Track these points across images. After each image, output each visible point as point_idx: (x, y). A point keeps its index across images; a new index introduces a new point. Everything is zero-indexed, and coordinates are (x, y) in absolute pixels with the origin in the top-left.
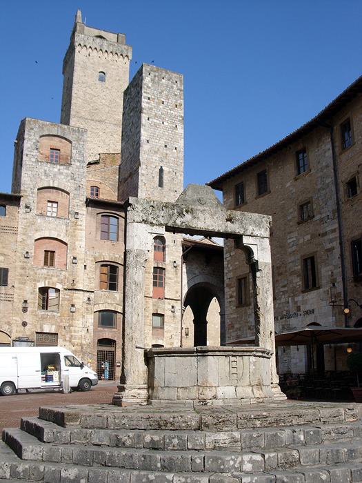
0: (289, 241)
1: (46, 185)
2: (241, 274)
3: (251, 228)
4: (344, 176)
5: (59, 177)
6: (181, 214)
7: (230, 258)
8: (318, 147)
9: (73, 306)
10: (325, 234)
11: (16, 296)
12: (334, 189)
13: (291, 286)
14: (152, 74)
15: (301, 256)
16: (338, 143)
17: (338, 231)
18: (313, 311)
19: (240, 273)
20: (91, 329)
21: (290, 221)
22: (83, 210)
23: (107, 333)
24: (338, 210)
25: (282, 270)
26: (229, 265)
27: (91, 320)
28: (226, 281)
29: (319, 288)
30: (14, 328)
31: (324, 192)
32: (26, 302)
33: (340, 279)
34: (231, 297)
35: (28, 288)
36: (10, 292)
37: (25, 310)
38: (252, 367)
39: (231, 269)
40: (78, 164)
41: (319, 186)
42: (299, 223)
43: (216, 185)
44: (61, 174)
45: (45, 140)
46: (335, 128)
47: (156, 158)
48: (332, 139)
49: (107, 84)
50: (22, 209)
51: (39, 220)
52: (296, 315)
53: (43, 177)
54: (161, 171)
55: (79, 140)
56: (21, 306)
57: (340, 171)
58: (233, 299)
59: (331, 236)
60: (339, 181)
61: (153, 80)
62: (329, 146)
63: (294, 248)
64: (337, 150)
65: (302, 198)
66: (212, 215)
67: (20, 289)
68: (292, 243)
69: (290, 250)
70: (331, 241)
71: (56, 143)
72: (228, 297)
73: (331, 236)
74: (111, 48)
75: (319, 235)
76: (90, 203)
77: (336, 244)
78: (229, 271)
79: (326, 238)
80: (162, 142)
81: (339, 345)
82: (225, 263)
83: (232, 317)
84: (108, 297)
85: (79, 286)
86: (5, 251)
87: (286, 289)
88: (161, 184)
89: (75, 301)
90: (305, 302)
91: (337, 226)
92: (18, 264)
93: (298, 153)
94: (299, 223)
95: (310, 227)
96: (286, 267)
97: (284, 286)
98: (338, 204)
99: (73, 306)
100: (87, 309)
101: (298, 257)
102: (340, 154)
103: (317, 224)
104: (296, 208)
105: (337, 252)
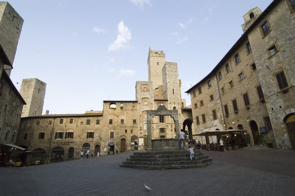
1: (144, 97)
3: (173, 113)
4: (221, 88)
5: (146, 95)
6: (158, 112)
9: (153, 128)
10: (217, 104)
11: (138, 126)
12: (218, 91)
13: (210, 118)
14: (168, 64)
16: (218, 78)
18: (216, 125)
19: (197, 116)
20: (158, 133)
22: (153, 103)
23: (163, 134)
24: (220, 97)
25: (207, 114)
27: (158, 131)
28: (193, 118)
29: (217, 119)
30: (139, 135)
31: (216, 92)
32: (141, 128)
33: (222, 116)
34: (195, 122)
35: (141, 124)
36: (137, 125)
37: (141, 130)
38: (172, 143)
40: (151, 91)
41: (215, 91)
43: (188, 92)
44: (147, 94)
45: (142, 86)
46: (217, 74)
47: (171, 86)
48: (217, 78)
49: (159, 65)
50: (138, 104)
51: (143, 106)
52: (212, 127)
53: (143, 95)
54: (173, 90)
55: (151, 85)
56: (140, 129)
57: (219, 86)
58: (196, 123)
59: (219, 104)
60: (219, 89)
61: (169, 66)
62: (216, 79)
64: (218, 80)
65: (211, 94)
66: (164, 112)
67: (139, 124)
69: (209, 109)
70: (219, 106)
71: (145, 86)
73: (219, 104)
74: (160, 55)
76: (155, 100)
77: (220, 106)
79: (218, 105)
80: (173, 82)
81: (225, 135)
82: (193, 113)
84: (162, 125)
85: (154, 122)
86: (135, 115)
87: (209, 119)
88: (173, 93)
89: (153, 126)
90: (214, 123)
91: (220, 101)
92: (138, 118)
93: (208, 82)
94: (210, 101)
95: (213, 102)
97: (208, 119)
98: (220, 95)
99: (153, 128)
100: (157, 128)
104: (209, 97)
105: (221, 109)
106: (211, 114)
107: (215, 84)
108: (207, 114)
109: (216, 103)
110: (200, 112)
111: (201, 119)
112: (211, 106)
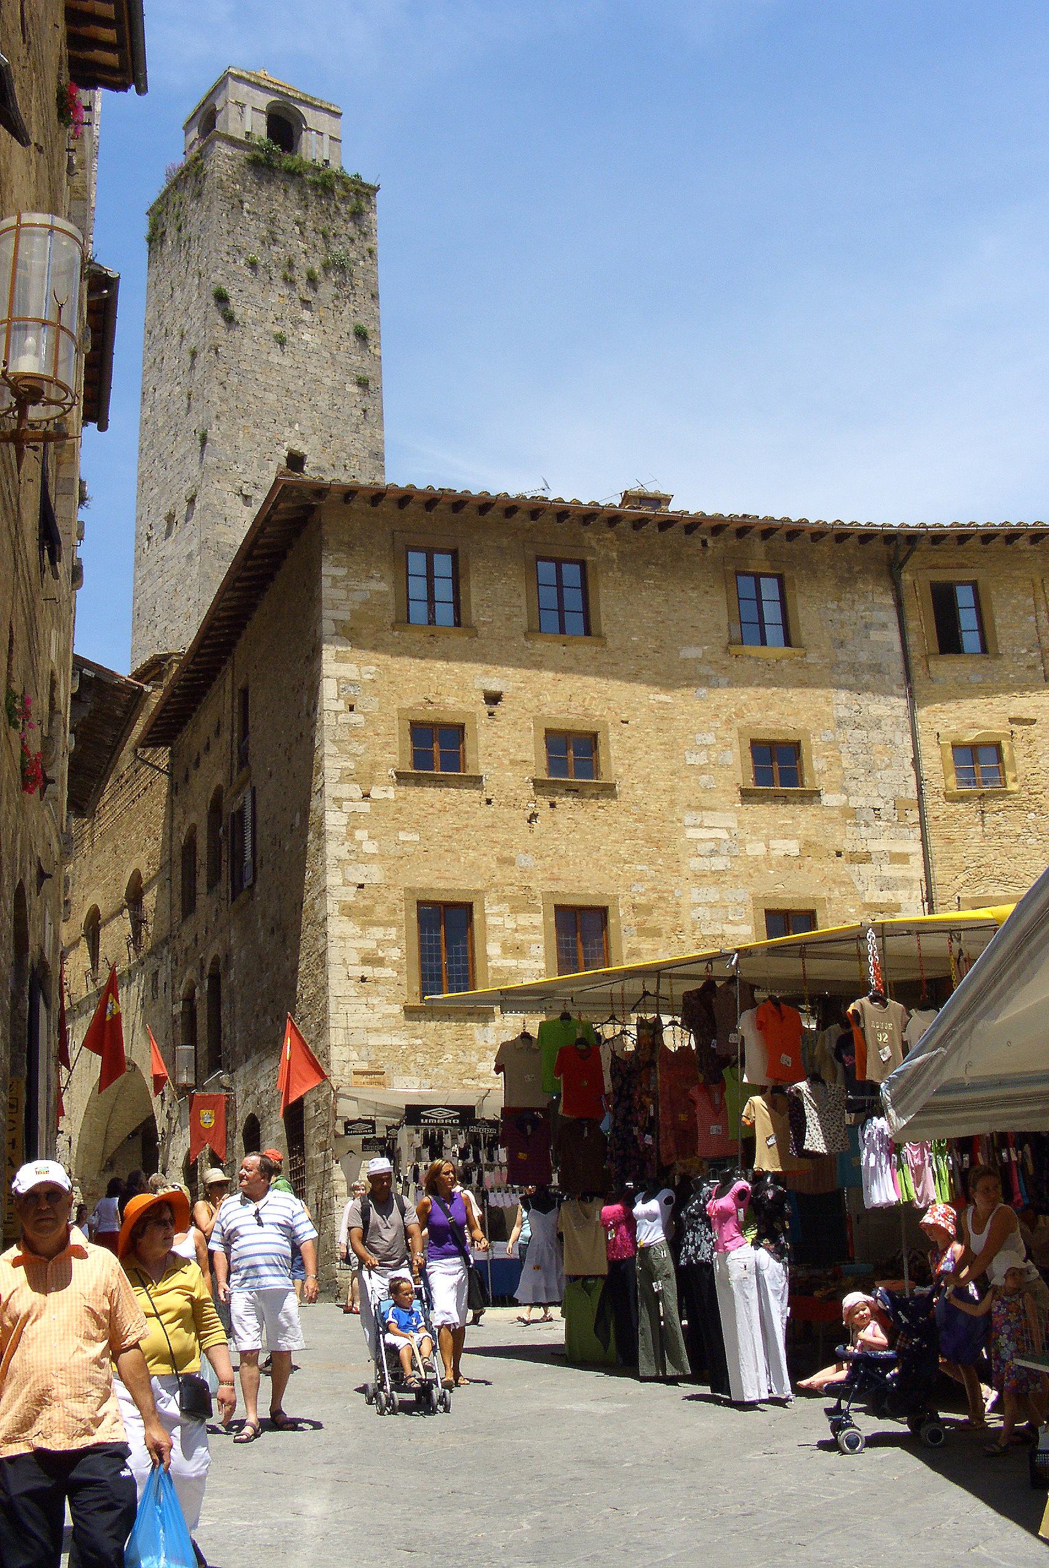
0: (691, 833)
2: (442, 885)
7: (365, 807)
8: (839, 600)
10: (866, 858)
15: (755, 899)
17: (917, 862)
21: (702, 770)
25: (656, 919)
26: (360, 835)
39: (370, 847)
42: (746, 795)
48: (899, 605)
58: (388, 972)
59: (891, 871)
62: (889, 616)
63: (719, 863)
64: (912, 639)
68: (711, 845)
69: (695, 863)
70: (887, 884)
72: (354, 958)
75: (839, 854)
78: (359, 857)
79: (866, 869)
83: (374, 1040)
96: (677, 915)
101: (743, 894)
102: (927, 657)
103: (831, 820)
106: (729, 930)
107: (864, 657)
108: (656, 919)
109: (847, 846)
110: (525, 860)
111: (517, 950)
112: (757, 849)
